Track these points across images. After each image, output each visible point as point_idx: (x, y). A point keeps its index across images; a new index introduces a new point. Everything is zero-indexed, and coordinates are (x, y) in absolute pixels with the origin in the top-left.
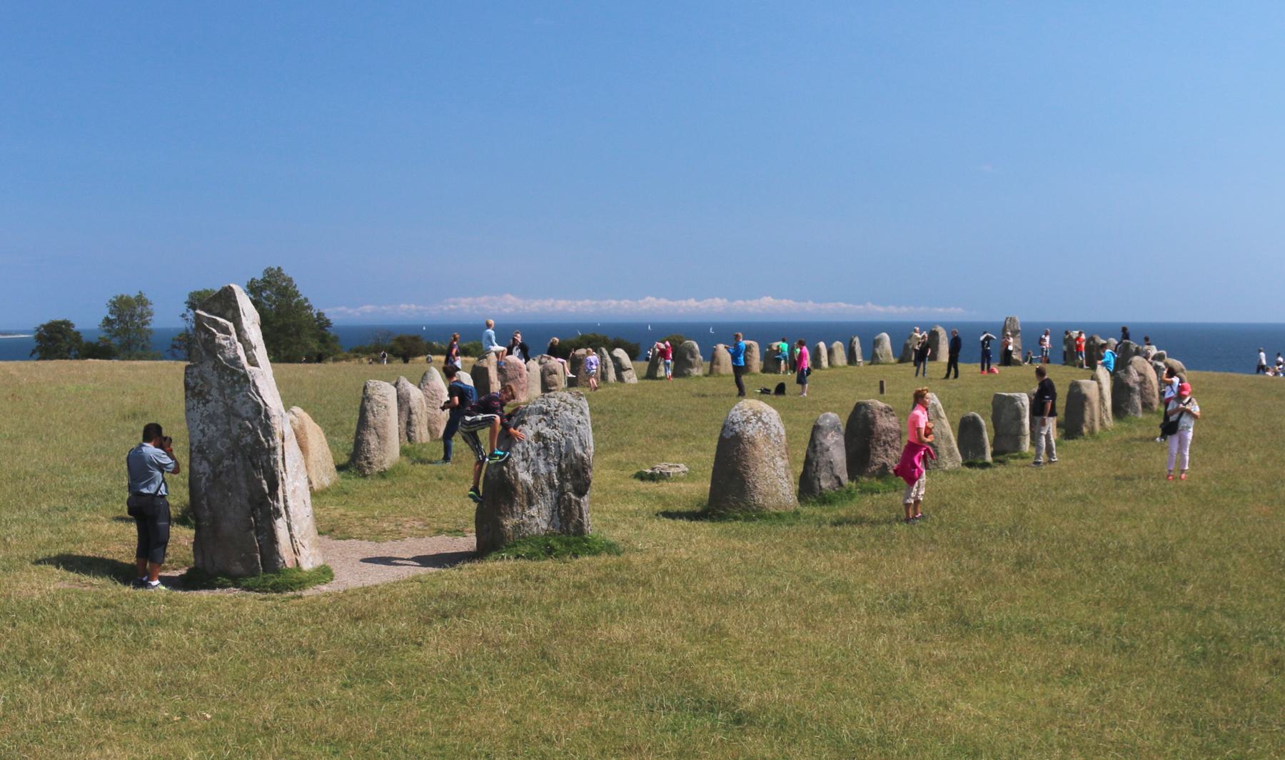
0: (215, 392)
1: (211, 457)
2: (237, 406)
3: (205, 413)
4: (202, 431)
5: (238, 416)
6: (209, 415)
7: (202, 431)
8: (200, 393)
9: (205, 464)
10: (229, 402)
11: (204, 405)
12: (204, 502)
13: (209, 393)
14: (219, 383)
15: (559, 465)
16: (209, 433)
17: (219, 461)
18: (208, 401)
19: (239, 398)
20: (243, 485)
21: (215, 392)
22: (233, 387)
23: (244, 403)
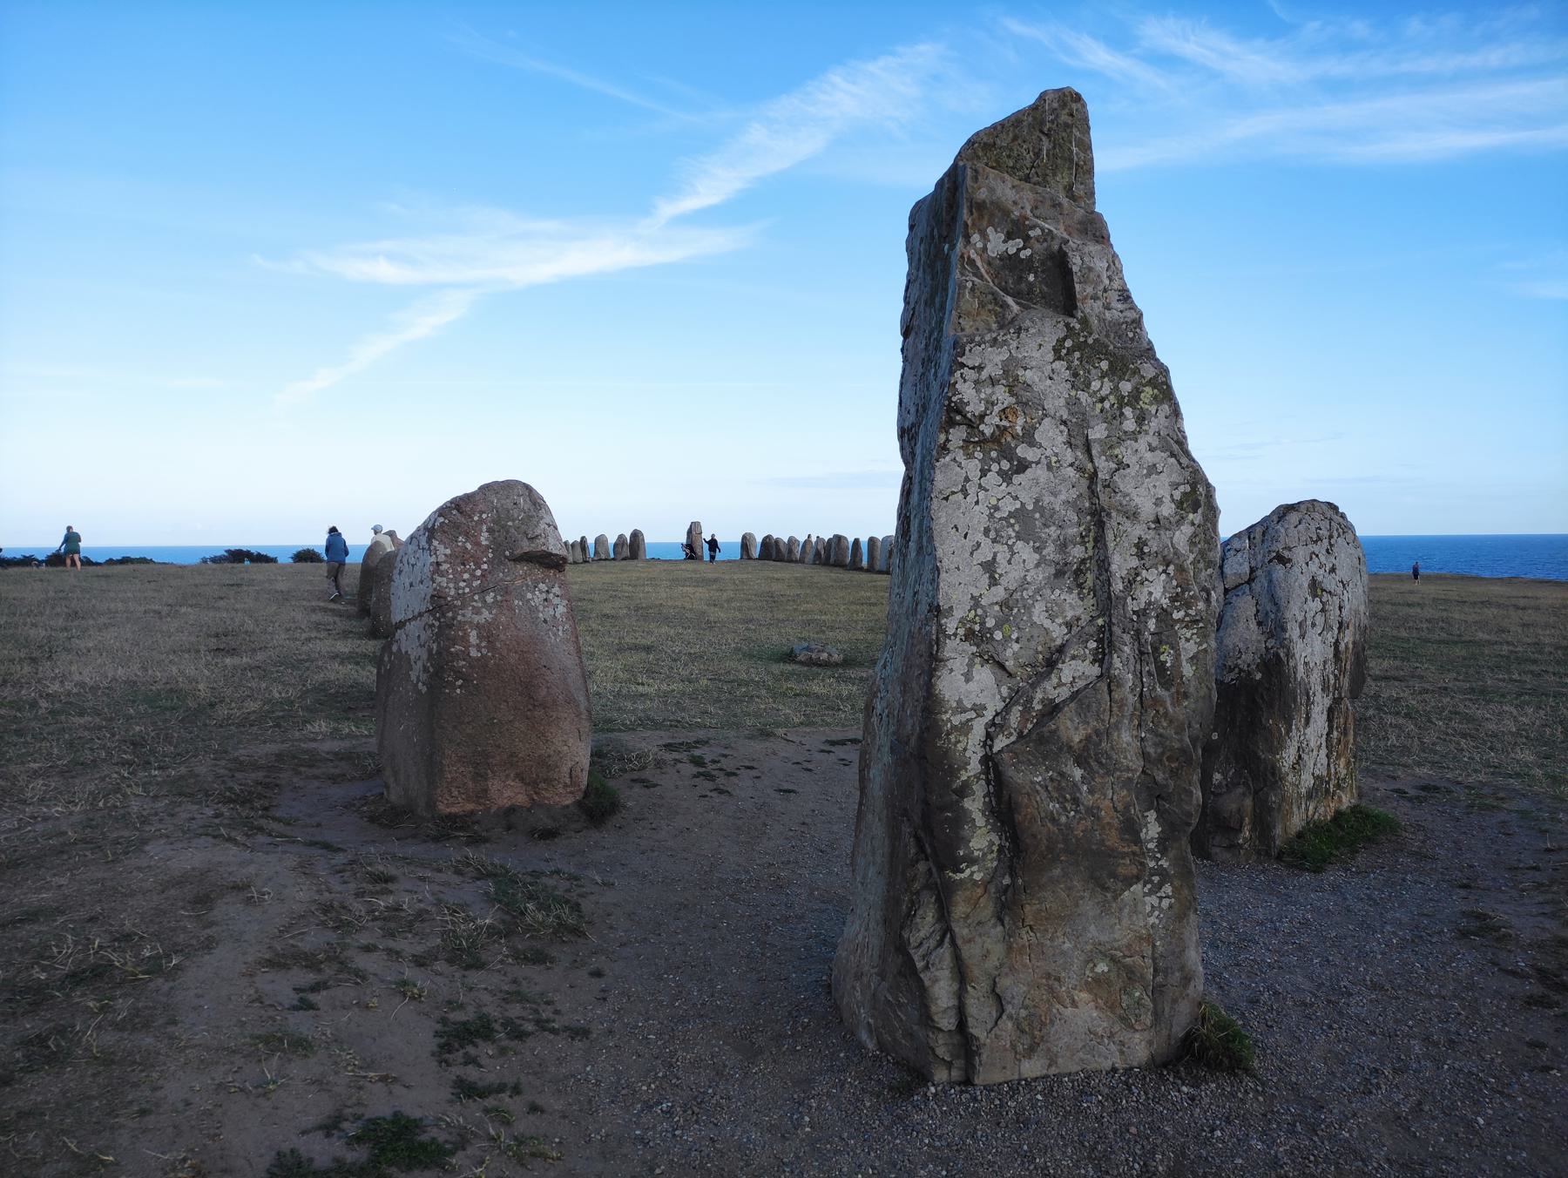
0: (1051, 436)
1: (1011, 654)
2: (1125, 483)
3: (1008, 506)
4: (989, 567)
5: (1133, 515)
6: (1020, 514)
7: (989, 567)
8: (995, 439)
9: (985, 674)
10: (1104, 465)
11: (1006, 477)
12: (974, 805)
13: (1028, 437)
14: (1072, 403)
15: (1337, 644)
16: (1011, 575)
17: (1052, 660)
18: (1022, 466)
19: (1139, 452)
20: (1126, 737)
21: (1051, 436)
22: (1115, 417)
23: (1153, 470)
